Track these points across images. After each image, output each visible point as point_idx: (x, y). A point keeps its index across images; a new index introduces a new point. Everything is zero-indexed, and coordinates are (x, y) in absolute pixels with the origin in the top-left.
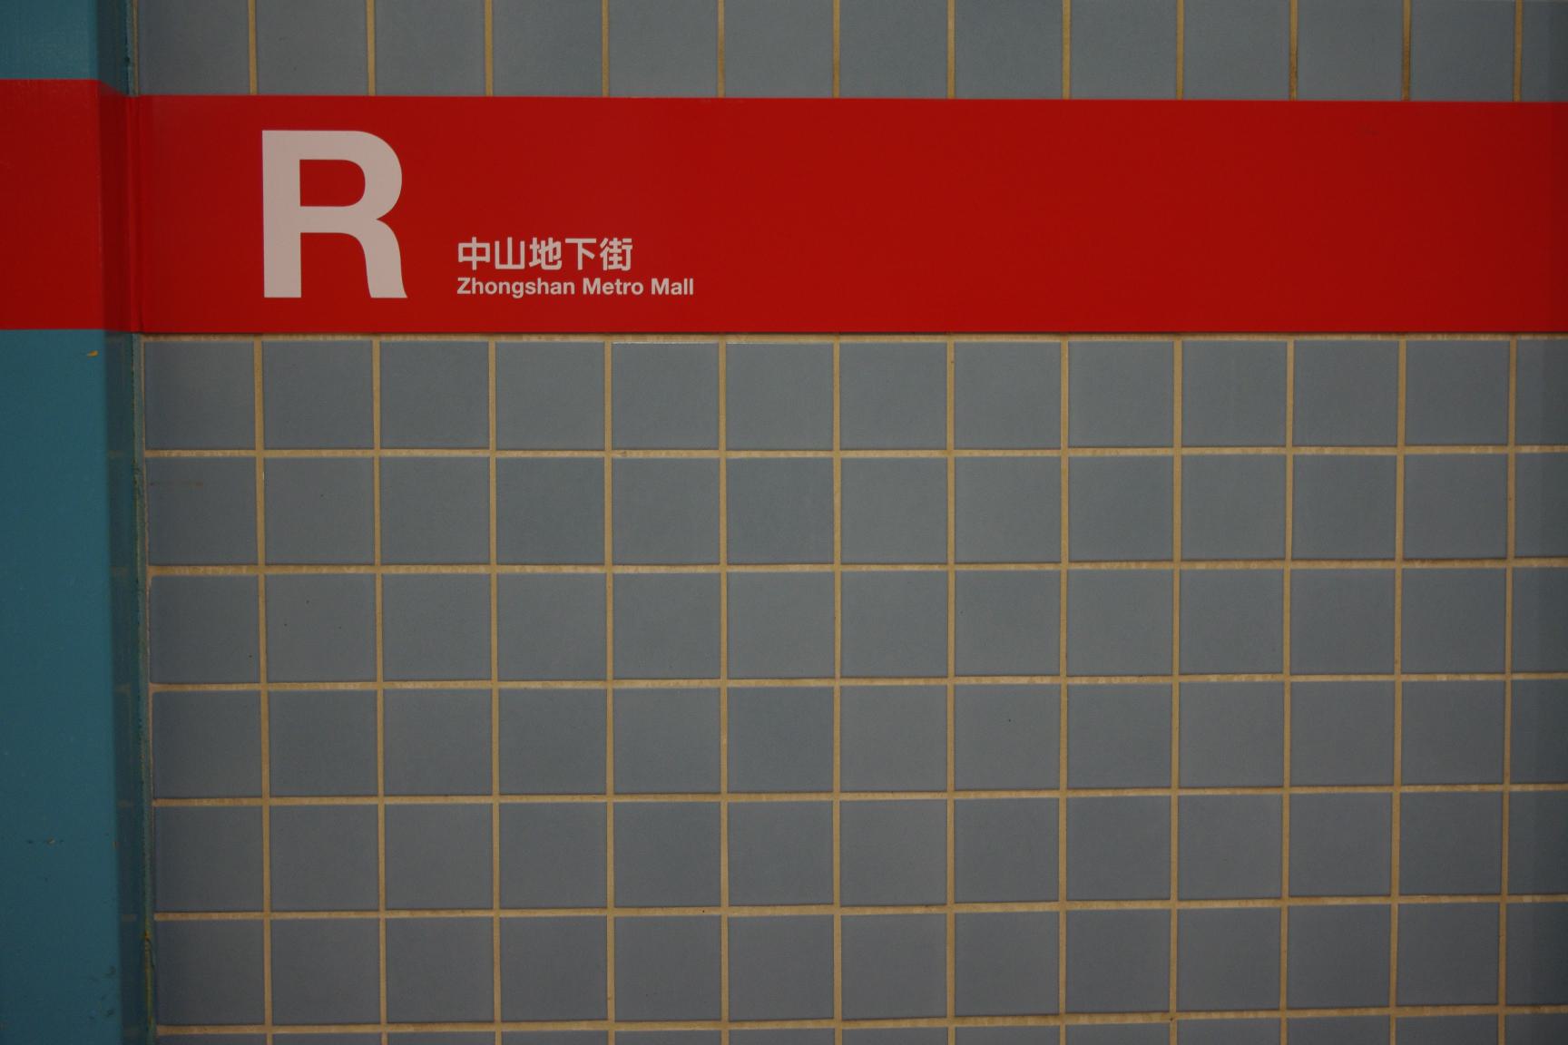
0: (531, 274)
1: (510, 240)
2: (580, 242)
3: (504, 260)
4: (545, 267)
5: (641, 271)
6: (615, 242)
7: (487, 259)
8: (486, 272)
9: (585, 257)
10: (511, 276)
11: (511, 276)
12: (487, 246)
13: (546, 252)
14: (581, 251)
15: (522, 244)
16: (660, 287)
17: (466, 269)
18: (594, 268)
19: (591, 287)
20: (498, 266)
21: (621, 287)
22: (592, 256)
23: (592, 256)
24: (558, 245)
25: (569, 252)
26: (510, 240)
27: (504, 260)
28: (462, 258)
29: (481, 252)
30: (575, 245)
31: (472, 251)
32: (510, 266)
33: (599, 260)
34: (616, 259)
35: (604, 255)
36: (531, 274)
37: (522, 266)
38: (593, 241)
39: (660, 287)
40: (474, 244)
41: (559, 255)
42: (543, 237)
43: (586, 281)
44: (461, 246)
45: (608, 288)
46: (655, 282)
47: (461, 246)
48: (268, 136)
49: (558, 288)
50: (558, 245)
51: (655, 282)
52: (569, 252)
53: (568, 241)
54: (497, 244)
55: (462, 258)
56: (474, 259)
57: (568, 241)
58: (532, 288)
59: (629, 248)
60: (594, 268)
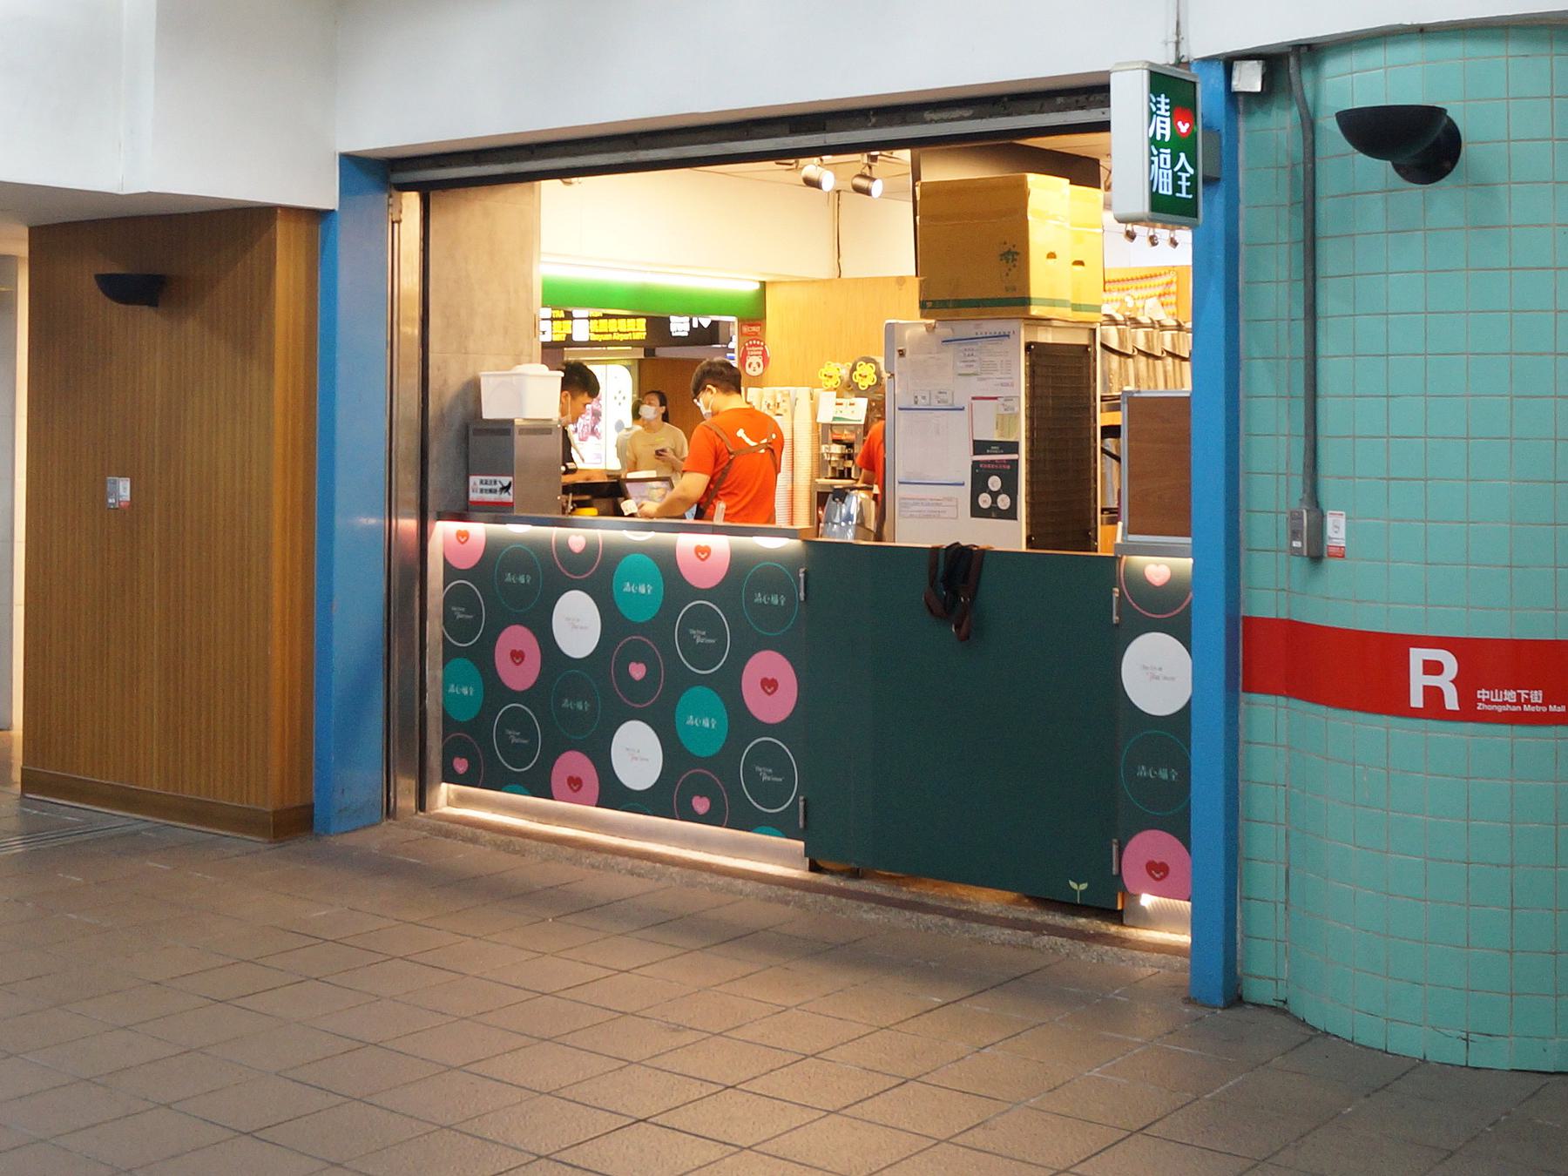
0: (1504, 703)
1: (1496, 691)
2: (1522, 692)
3: (1494, 697)
4: (1510, 701)
5: (1545, 703)
6: (1536, 692)
7: (1488, 697)
8: (1488, 702)
9: (1525, 698)
10: (1497, 703)
11: (1497, 703)
12: (1488, 692)
13: (1510, 695)
14: (1523, 695)
15: (1501, 692)
16: (1553, 708)
17: (1480, 700)
18: (1528, 702)
19: (1527, 708)
20: (1492, 700)
21: (1538, 709)
22: (1527, 697)
23: (1527, 697)
24: (1515, 693)
25: (1519, 696)
26: (1496, 691)
27: (1494, 697)
28: (1479, 697)
29: (1486, 694)
30: (1520, 694)
31: (1483, 694)
32: (1496, 700)
33: (1530, 699)
34: (1536, 698)
35: (1531, 697)
36: (1504, 703)
37: (1501, 700)
38: (1527, 692)
39: (1553, 708)
40: (1483, 691)
41: (1515, 696)
42: (1509, 690)
43: (1525, 706)
44: (1479, 692)
45: (1533, 709)
46: (1550, 706)
47: (1479, 692)
48: (1412, 650)
49: (1515, 709)
50: (1515, 693)
51: (1550, 706)
52: (1519, 696)
53: (1519, 691)
54: (1492, 692)
55: (1479, 697)
56: (1483, 697)
57: (1519, 691)
58: (1507, 708)
59: (1541, 695)
60: (1528, 702)
